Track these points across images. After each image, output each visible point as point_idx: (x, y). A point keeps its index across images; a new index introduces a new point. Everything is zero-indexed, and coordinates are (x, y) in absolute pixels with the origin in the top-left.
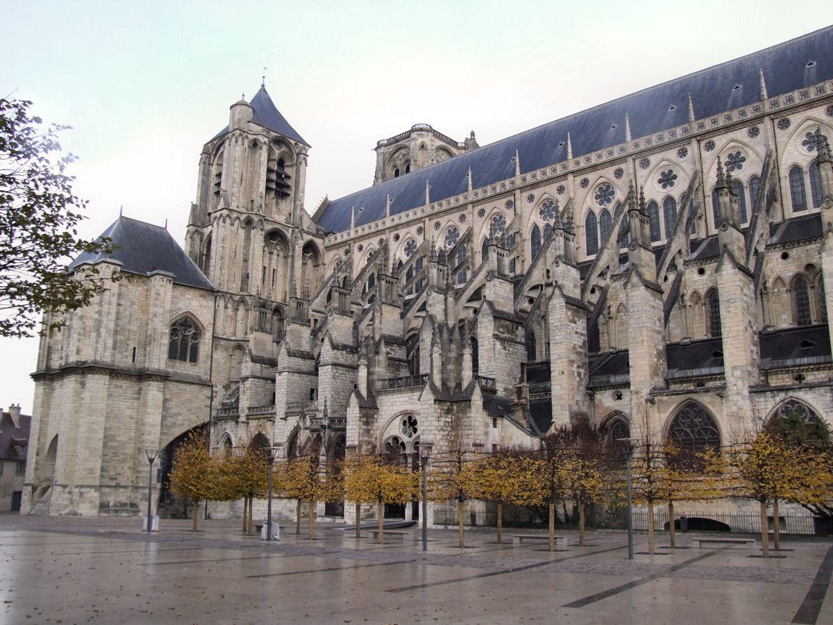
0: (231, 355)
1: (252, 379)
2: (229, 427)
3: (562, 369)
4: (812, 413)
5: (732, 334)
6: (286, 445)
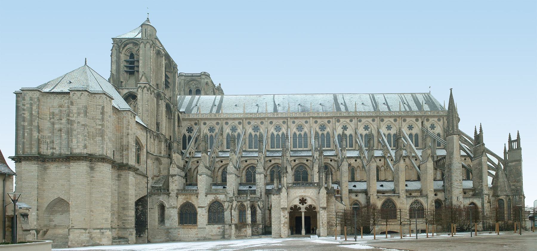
0: (153, 163)
1: (178, 176)
2: (162, 198)
3: (346, 185)
4: (421, 203)
5: (402, 181)
6: (207, 208)
